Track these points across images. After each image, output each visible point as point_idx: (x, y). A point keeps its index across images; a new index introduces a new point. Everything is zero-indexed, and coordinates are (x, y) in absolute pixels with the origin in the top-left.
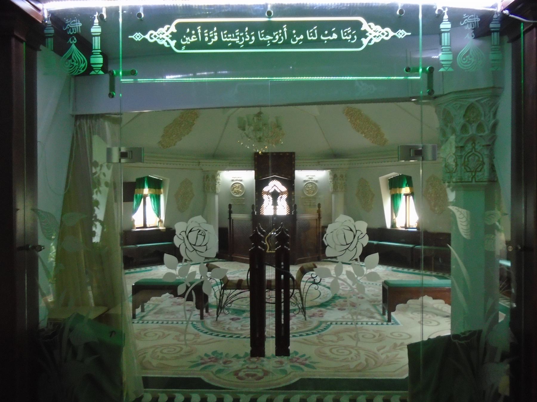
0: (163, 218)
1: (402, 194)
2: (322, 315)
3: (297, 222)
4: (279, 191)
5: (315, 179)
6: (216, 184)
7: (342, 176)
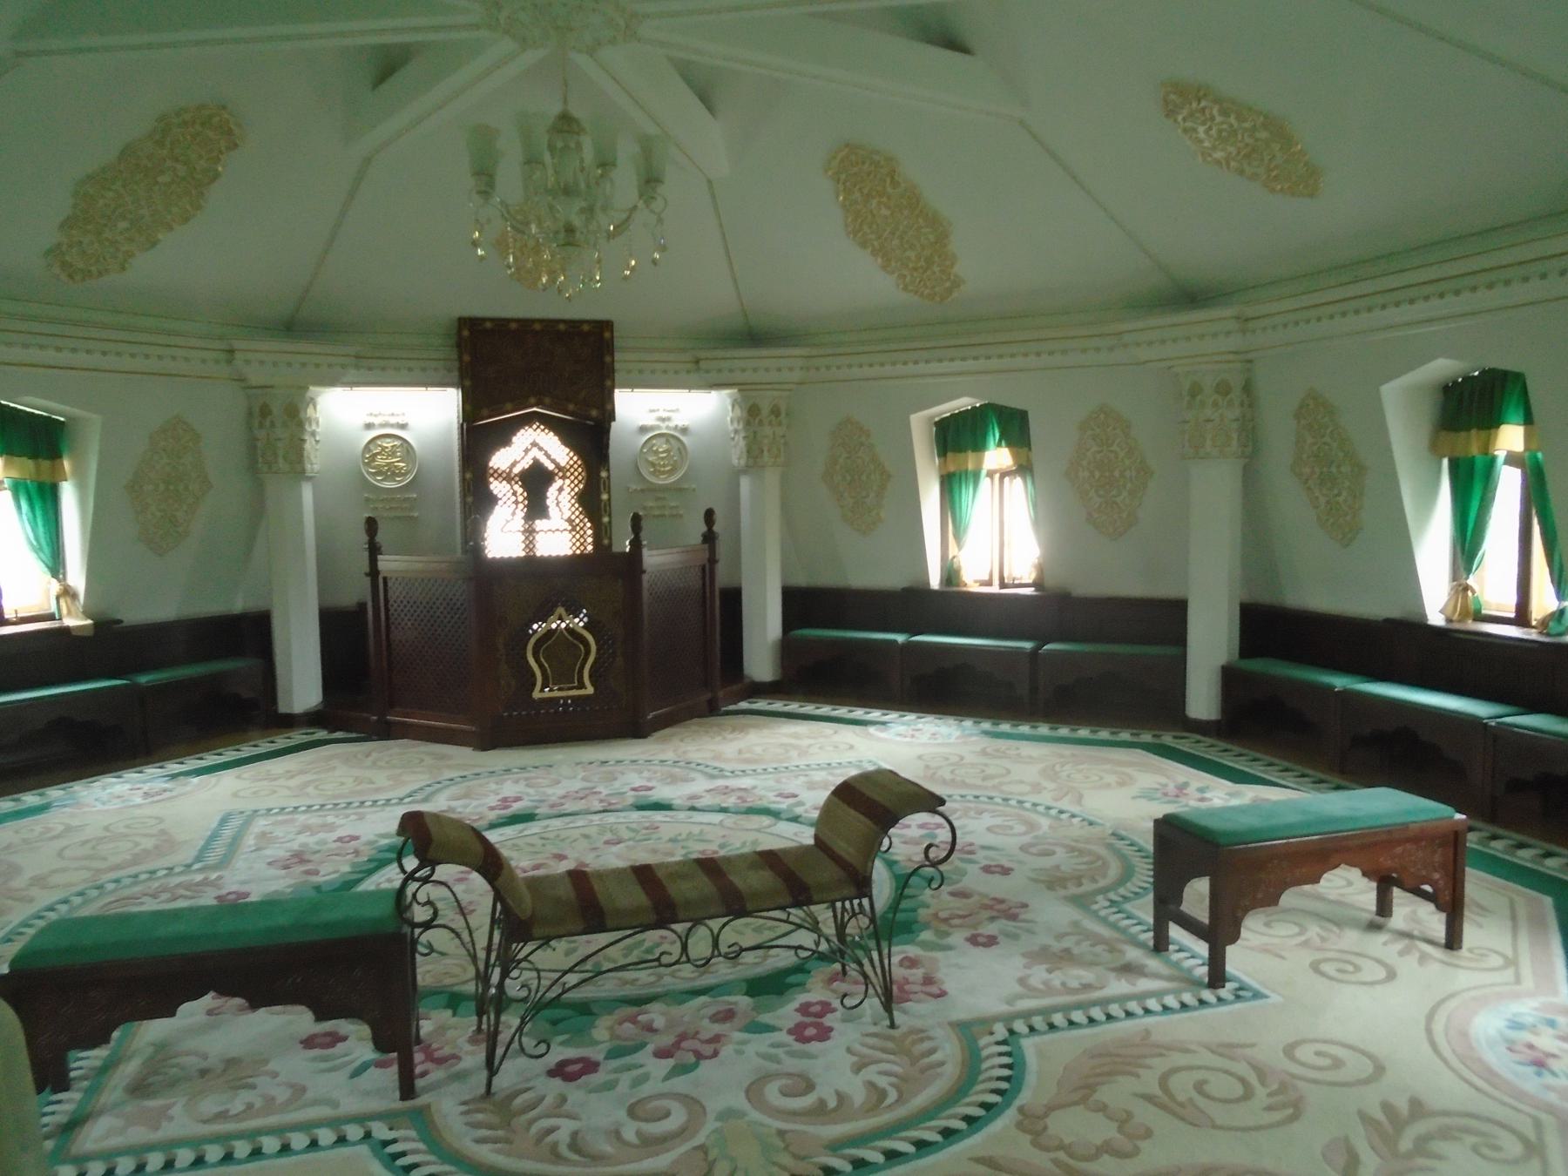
0: (77, 577)
1: (984, 473)
3: (645, 577)
4: (551, 467)
5: (679, 420)
6: (304, 441)
7: (776, 412)
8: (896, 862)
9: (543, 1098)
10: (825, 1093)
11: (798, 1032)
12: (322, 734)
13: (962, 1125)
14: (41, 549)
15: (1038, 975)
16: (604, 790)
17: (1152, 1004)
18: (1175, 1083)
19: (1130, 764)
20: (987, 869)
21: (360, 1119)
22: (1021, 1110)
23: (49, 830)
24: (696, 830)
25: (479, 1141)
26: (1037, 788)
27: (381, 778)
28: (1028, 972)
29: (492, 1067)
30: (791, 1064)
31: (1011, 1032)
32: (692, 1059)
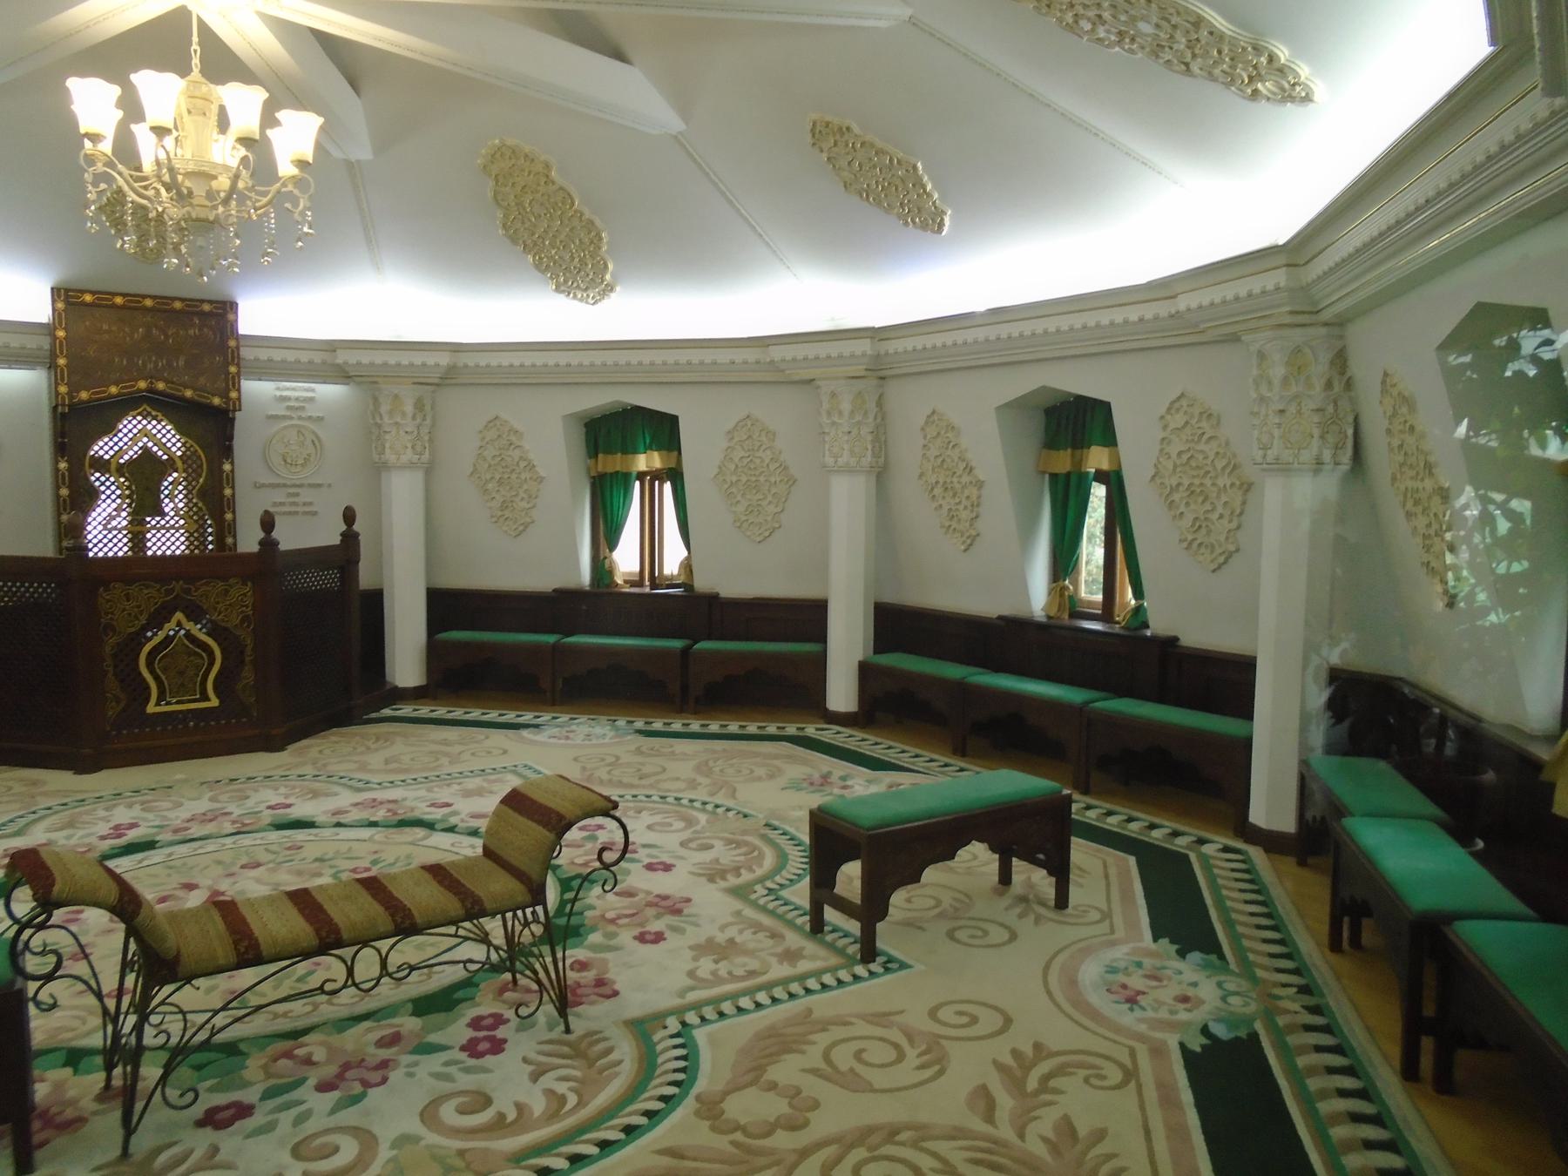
9: (192, 1151)
10: (504, 1104)
11: (471, 1048)
13: (643, 1120)
15: (706, 966)
16: (236, 811)
17: (812, 984)
18: (836, 1055)
19: (776, 757)
20: (650, 867)
22: (698, 1098)
24: (344, 847)
26: (693, 785)
29: (129, 1128)
30: (465, 1081)
31: (684, 1024)
32: (357, 1088)
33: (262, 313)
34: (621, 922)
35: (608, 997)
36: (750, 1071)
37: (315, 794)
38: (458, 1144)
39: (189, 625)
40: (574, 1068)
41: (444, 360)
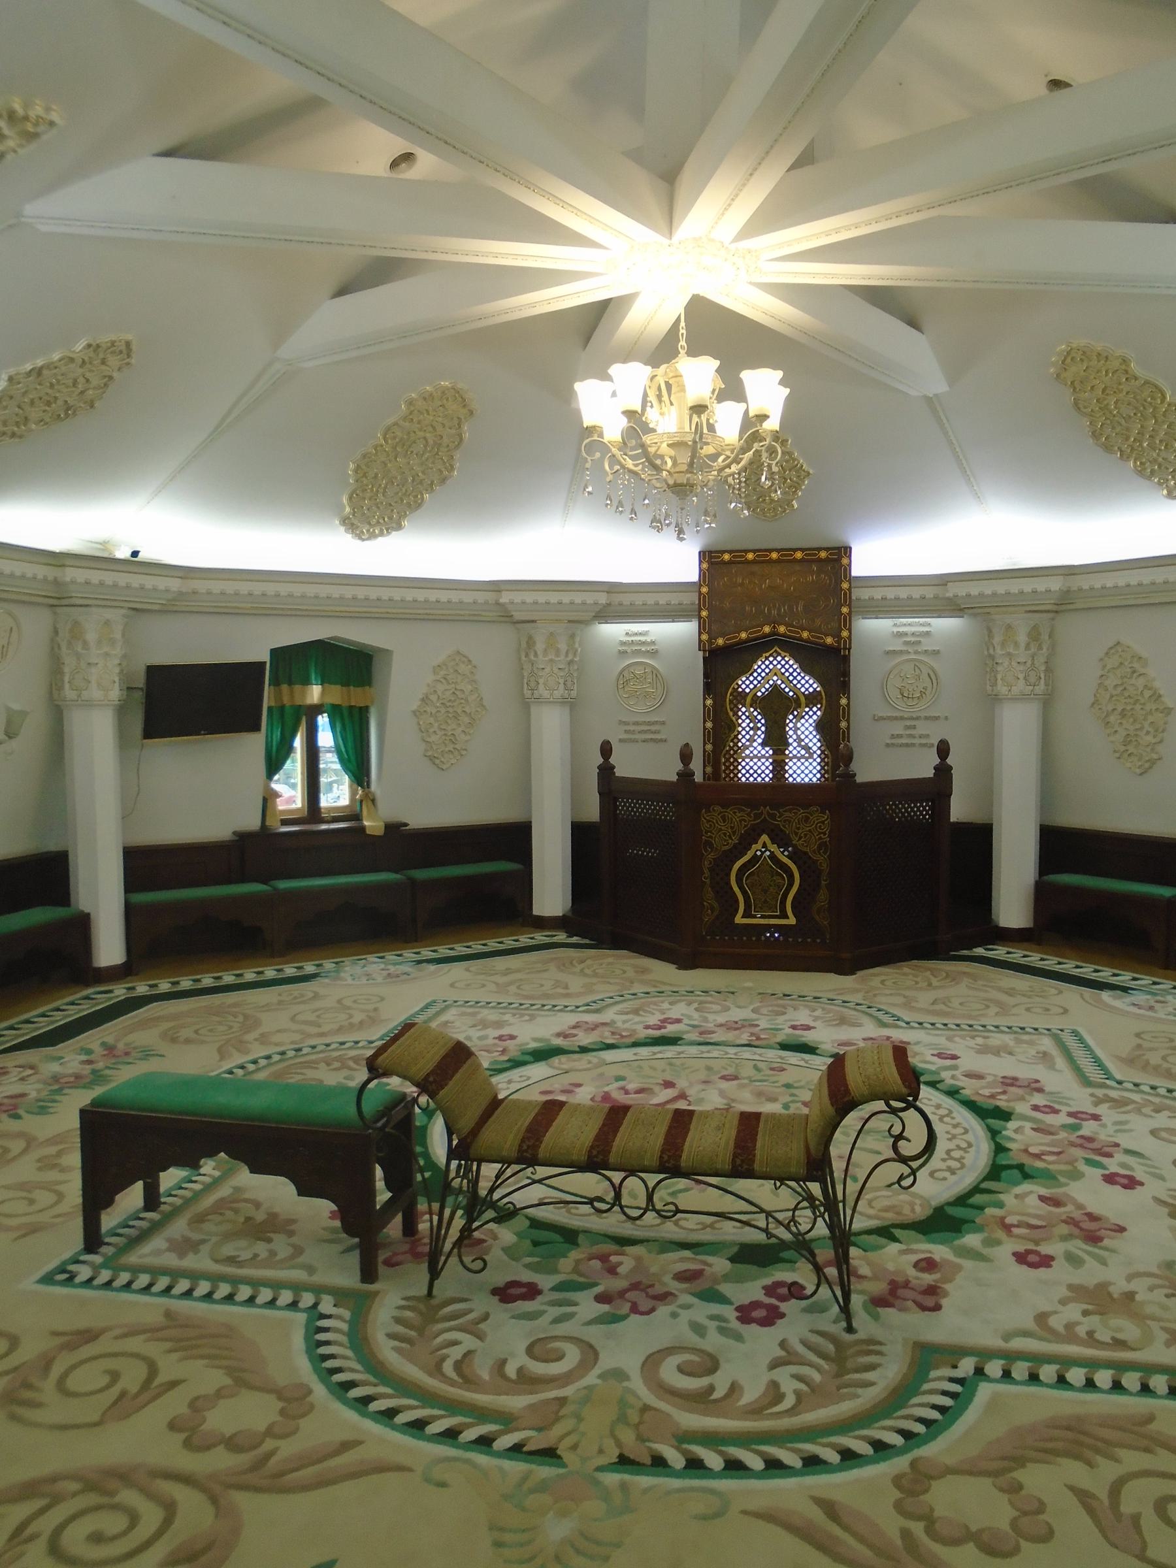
2: (930, 1299)
8: (1009, 1150)
9: (471, 1311)
11: (746, 1314)
12: (561, 937)
14: (349, 761)
15: (1073, 1312)
16: (763, 1023)
21: (318, 1290)
22: (913, 1464)
23: (302, 996)
25: (391, 1336)
27: (576, 983)
28: (1060, 1308)
30: (713, 1341)
31: (979, 1371)
33: (875, 554)
34: (1016, 1231)
35: (924, 1308)
36: (1003, 1458)
37: (843, 1021)
38: (647, 1396)
39: (773, 848)
40: (818, 1369)
41: (1055, 584)
